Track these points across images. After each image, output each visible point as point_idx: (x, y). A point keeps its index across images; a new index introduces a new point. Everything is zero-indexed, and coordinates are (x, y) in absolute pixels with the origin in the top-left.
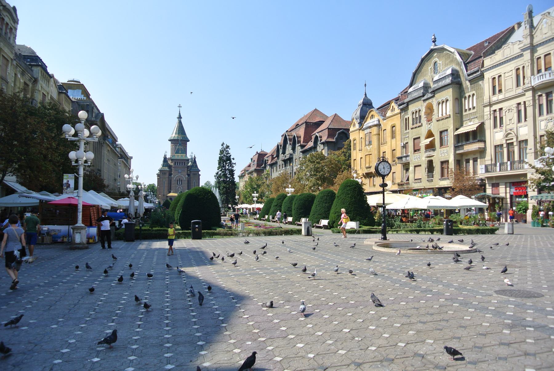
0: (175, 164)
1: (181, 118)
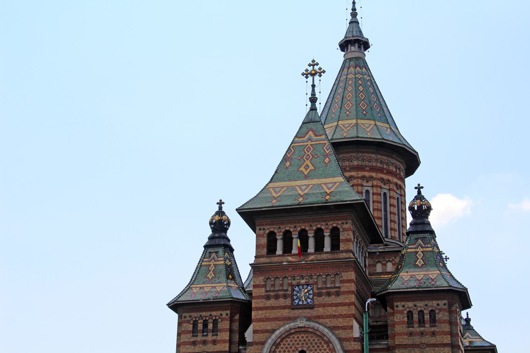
0: (271, 249)
1: (365, 45)
